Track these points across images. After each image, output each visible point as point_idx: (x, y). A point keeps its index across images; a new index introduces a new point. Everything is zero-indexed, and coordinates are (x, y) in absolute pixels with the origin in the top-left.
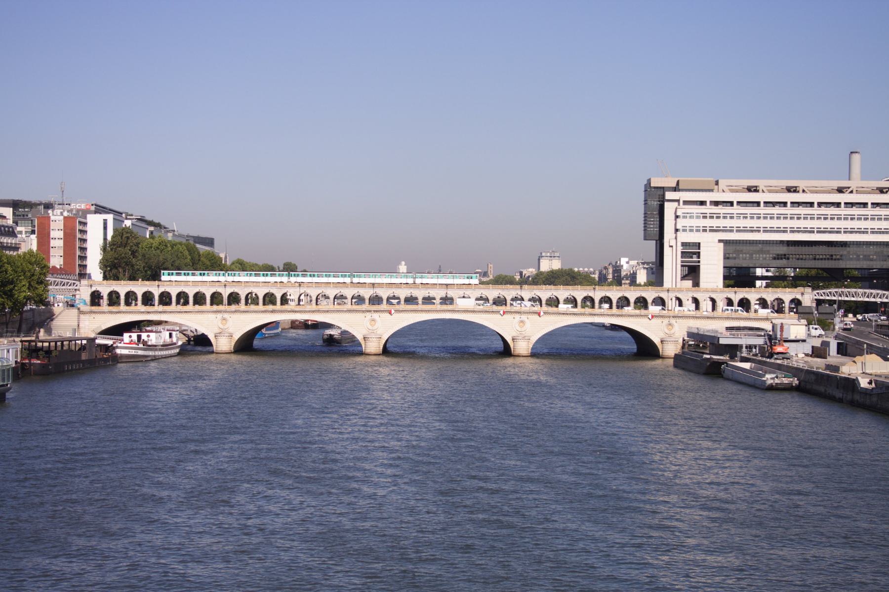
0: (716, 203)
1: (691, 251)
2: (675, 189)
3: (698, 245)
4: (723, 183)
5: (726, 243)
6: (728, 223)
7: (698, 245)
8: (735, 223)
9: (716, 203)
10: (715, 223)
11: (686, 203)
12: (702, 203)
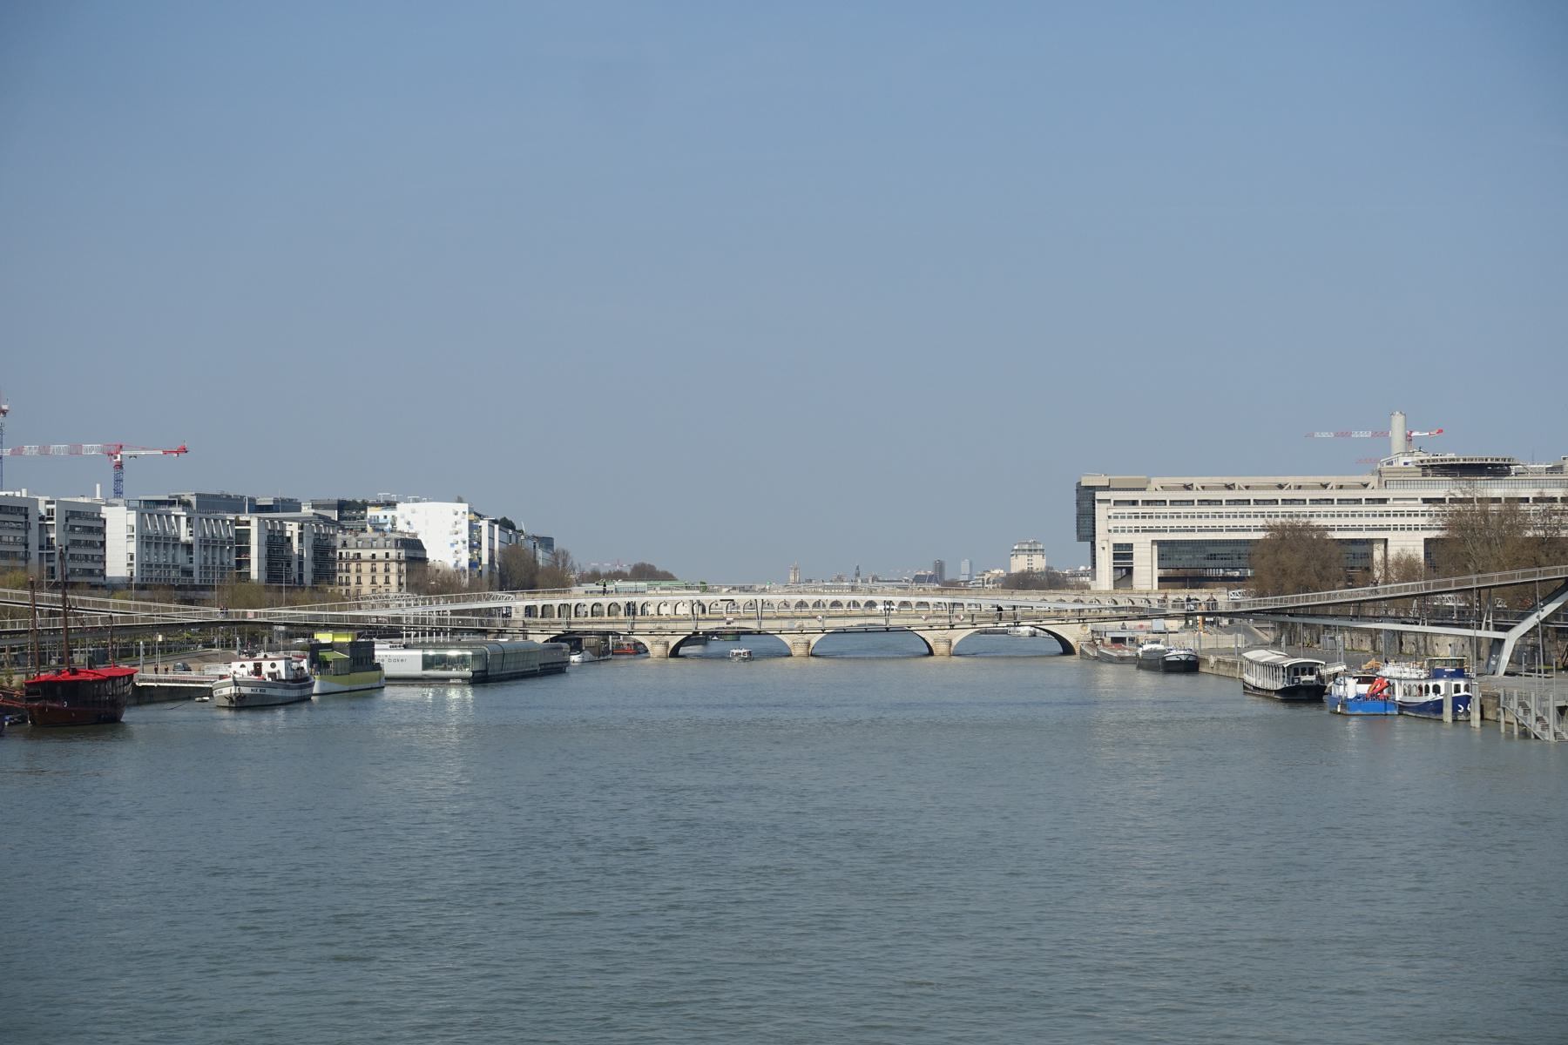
0: (1147, 503)
1: (1123, 554)
2: (1107, 488)
3: (1130, 546)
4: (1156, 482)
5: (1160, 543)
6: (1161, 523)
7: (1130, 546)
8: (1169, 523)
9: (1147, 503)
10: (1147, 523)
11: (1117, 503)
12: (1134, 503)
